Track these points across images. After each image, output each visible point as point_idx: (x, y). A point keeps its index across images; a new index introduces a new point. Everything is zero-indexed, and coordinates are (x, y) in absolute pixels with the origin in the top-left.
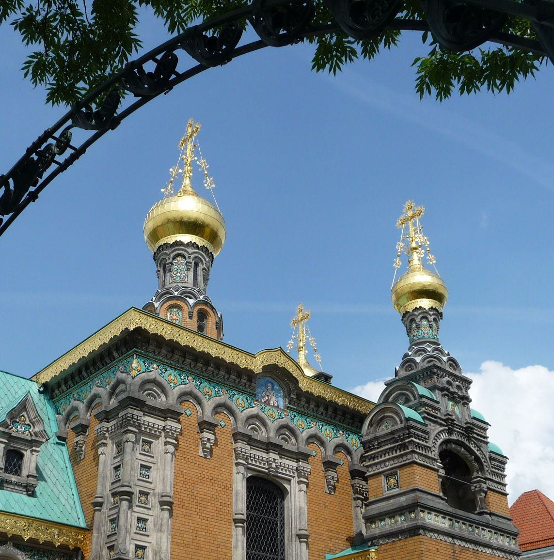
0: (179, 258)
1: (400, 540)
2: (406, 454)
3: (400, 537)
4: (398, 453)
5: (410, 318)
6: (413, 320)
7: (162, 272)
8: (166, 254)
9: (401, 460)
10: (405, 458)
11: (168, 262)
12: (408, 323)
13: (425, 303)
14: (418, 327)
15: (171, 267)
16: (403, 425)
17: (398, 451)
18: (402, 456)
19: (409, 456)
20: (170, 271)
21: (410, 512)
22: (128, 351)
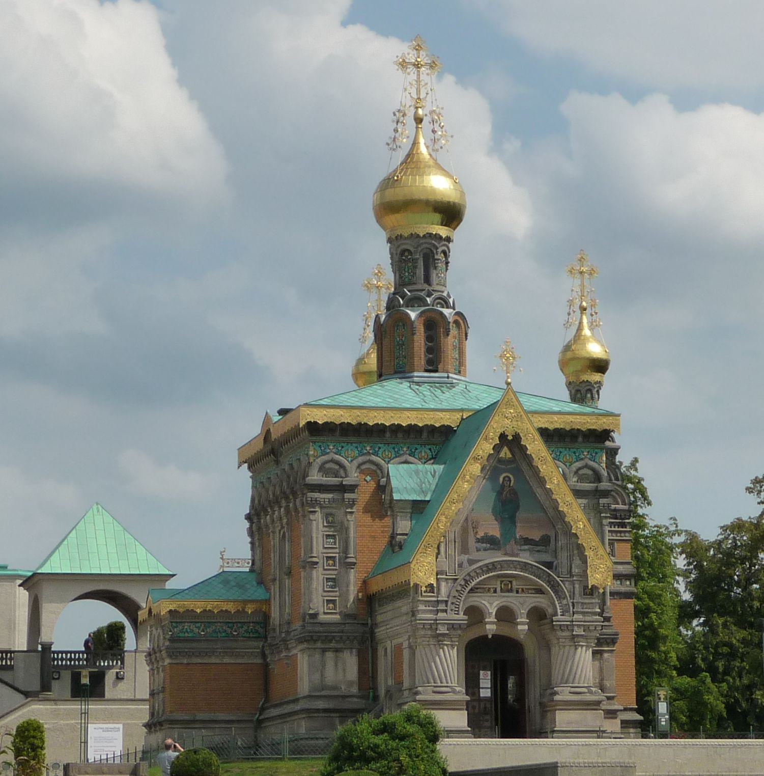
0: (442, 255)
1: (615, 599)
2: (625, 532)
3: (615, 597)
4: (616, 529)
5: (588, 387)
6: (590, 391)
7: (421, 263)
8: (434, 245)
9: (619, 535)
10: (623, 535)
11: (436, 257)
12: (583, 391)
13: (596, 377)
14: (592, 398)
15: (438, 263)
16: (626, 507)
17: (616, 527)
18: (621, 532)
19: (627, 534)
20: (435, 268)
21: (626, 579)
22: (595, 442)
